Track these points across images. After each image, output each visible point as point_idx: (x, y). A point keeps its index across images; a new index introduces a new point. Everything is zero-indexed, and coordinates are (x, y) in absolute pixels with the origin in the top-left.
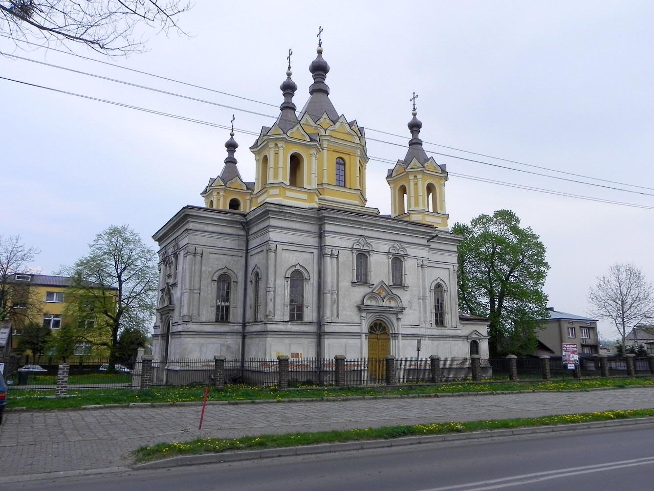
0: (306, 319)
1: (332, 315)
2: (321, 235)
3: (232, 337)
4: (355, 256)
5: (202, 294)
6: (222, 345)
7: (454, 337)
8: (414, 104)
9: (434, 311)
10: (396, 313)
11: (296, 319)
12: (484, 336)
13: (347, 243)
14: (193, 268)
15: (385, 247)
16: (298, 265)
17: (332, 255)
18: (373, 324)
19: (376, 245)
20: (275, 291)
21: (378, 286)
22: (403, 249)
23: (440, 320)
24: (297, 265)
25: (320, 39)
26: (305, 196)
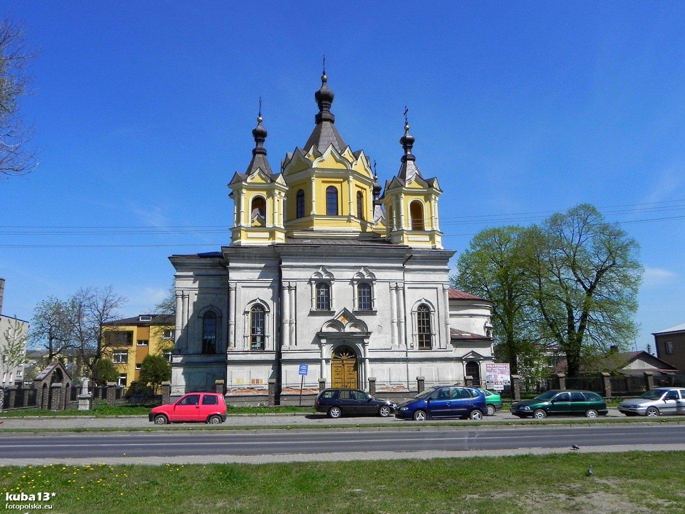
1: (291, 344)
6: (208, 373)
19: (336, 274)
23: (425, 340)
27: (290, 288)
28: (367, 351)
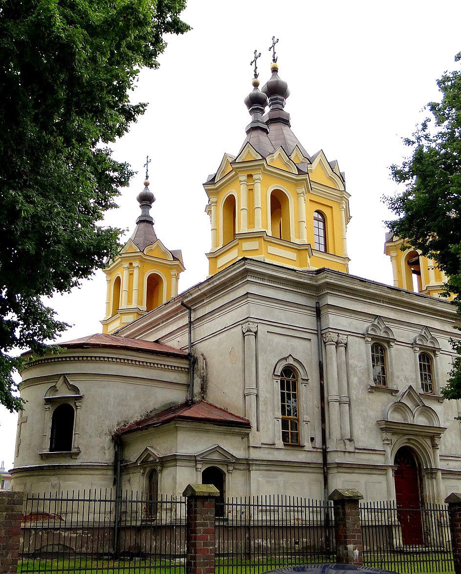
2: (318, 313)
4: (370, 346)
26: (292, 255)
28: (438, 458)
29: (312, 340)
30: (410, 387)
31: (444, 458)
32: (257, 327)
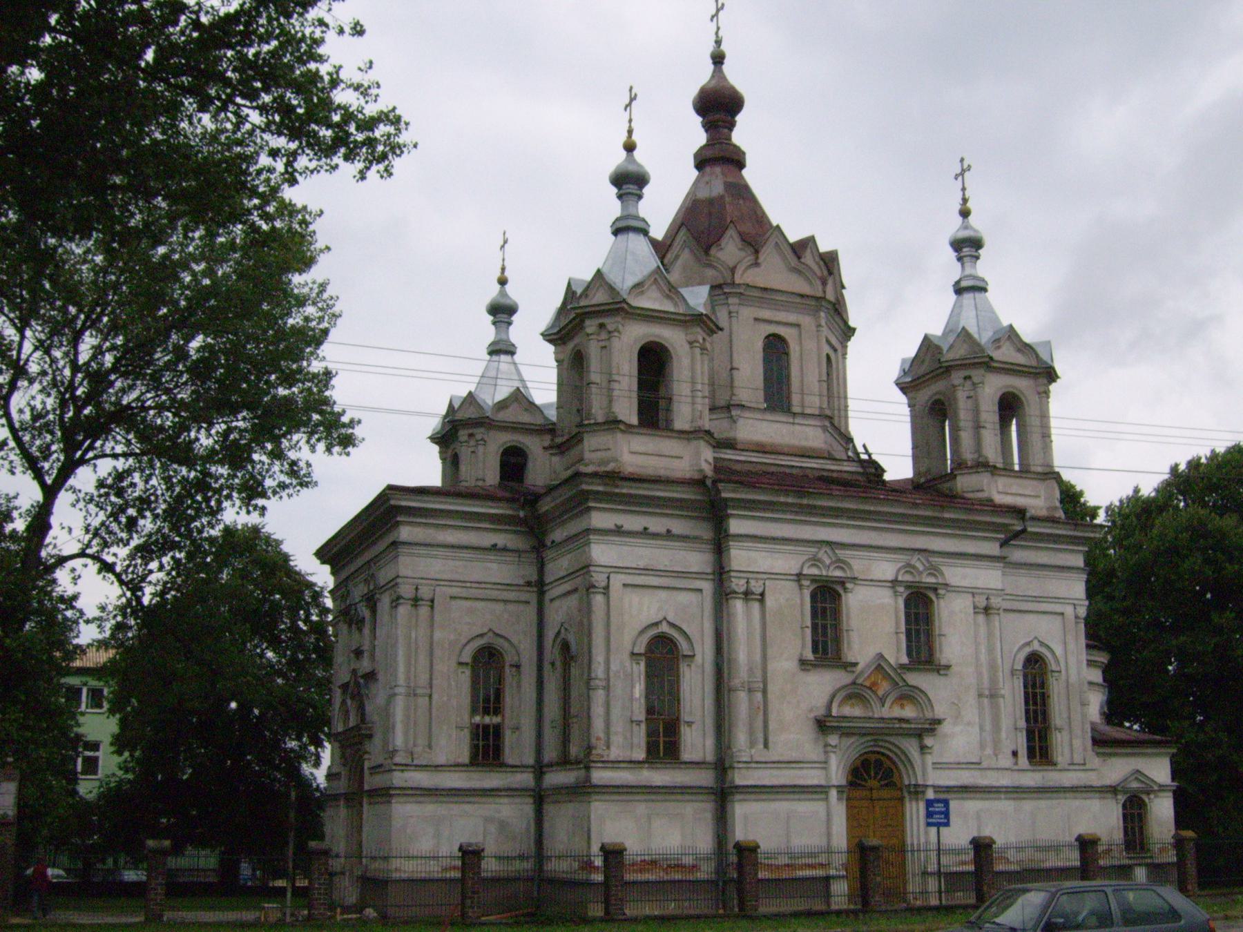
0: (686, 756)
1: (752, 744)
2: (720, 545)
3: (511, 800)
5: (435, 696)
6: (488, 820)
7: (1075, 790)
8: (964, 189)
9: (1022, 723)
10: (919, 734)
11: (662, 754)
12: (1160, 786)
13: (786, 562)
14: (413, 635)
15: (886, 569)
16: (664, 623)
17: (747, 594)
18: (859, 762)
19: (859, 564)
20: (607, 688)
21: (868, 666)
22: (934, 570)
24: (661, 622)
25: (718, 28)
27: (747, 594)
29: (704, 592)
30: (881, 656)
31: (937, 766)
32: (608, 578)
